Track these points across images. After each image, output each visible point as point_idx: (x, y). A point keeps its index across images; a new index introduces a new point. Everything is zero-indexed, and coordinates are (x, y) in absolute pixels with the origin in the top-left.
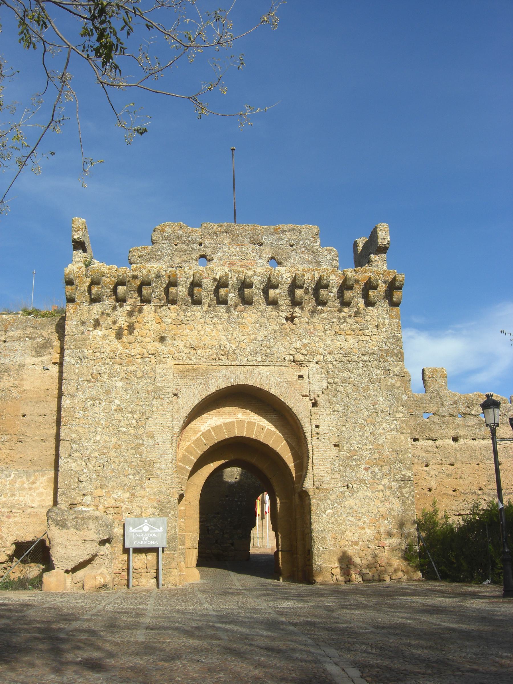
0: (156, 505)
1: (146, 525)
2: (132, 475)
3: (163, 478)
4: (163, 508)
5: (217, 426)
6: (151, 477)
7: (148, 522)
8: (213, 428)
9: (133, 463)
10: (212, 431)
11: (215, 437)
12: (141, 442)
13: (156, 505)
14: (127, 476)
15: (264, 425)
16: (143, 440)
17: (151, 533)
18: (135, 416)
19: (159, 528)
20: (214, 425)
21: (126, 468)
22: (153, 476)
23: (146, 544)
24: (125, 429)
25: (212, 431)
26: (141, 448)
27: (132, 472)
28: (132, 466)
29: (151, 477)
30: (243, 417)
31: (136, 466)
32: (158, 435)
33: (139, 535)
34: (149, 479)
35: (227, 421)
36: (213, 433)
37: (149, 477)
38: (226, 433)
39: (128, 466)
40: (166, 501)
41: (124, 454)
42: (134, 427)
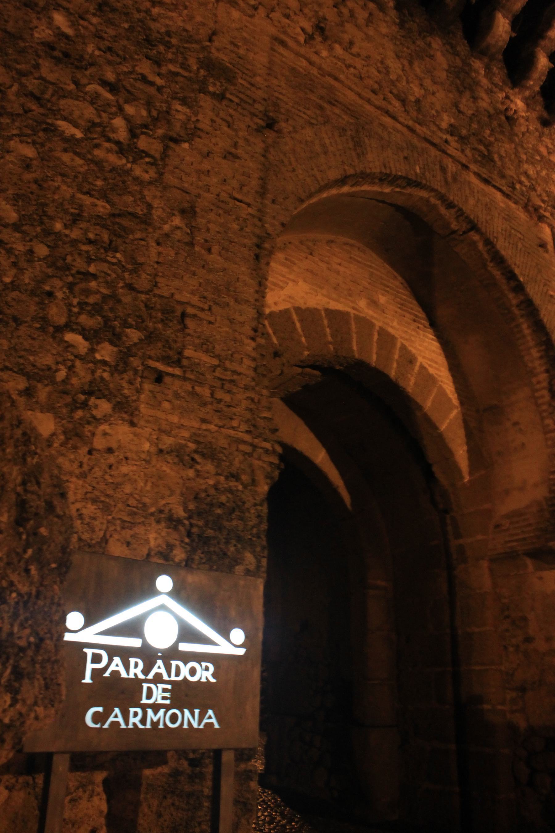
0: (180, 513)
1: (163, 607)
2: (84, 332)
3: (220, 394)
4: (210, 533)
5: (308, 309)
6: (170, 370)
7: (176, 593)
8: (298, 310)
9: (93, 284)
10: (295, 317)
11: (303, 339)
12: (140, 210)
13: (180, 513)
14: (59, 329)
15: (414, 351)
16: (150, 206)
17: (186, 657)
18: (130, 109)
19: (226, 635)
20: (301, 303)
21: (59, 295)
22: (177, 371)
23: (155, 724)
24: (79, 135)
25: (295, 317)
26: (138, 235)
27: (83, 319)
28: (87, 292)
29: (170, 370)
30: (371, 313)
31: (105, 298)
32: (212, 216)
33: (117, 664)
34: (159, 378)
35: (334, 305)
36: (298, 325)
37: (161, 366)
38: (330, 339)
39: (71, 287)
40: (223, 499)
41: (58, 226)
42: (118, 143)
